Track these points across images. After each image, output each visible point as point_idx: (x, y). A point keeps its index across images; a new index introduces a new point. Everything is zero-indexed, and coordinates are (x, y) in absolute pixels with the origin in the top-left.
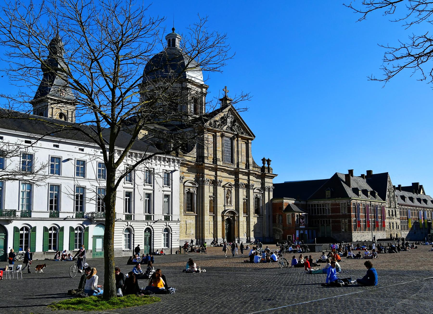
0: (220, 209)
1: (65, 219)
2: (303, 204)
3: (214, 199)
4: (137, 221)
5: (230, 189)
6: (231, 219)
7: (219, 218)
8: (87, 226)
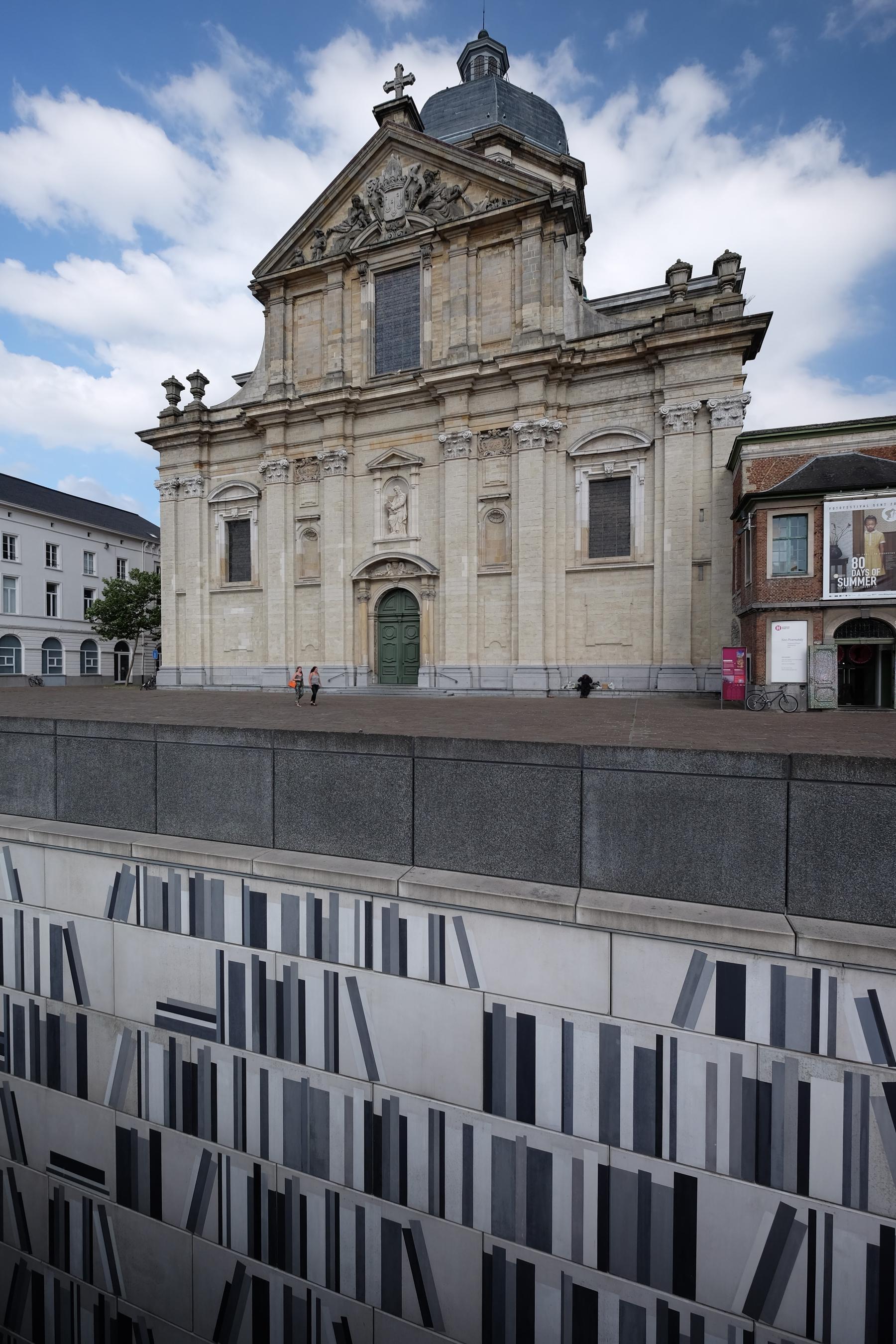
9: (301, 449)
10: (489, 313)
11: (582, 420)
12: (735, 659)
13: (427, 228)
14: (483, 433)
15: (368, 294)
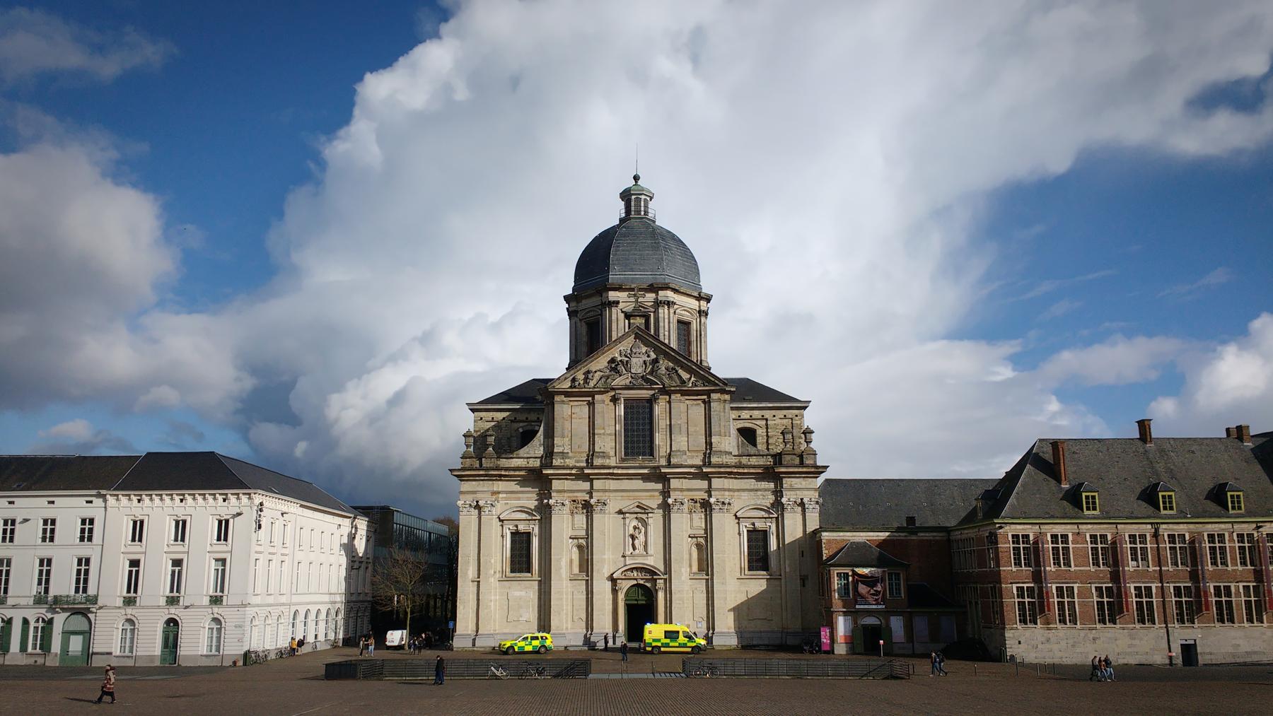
0: (608, 560)
1: (14, 607)
2: (931, 540)
4: (143, 607)
5: (644, 516)
6: (649, 585)
7: (602, 589)
8: (52, 616)
9: (576, 494)
10: (692, 435)
11: (743, 497)
12: (826, 632)
13: (658, 384)
14: (693, 500)
15: (621, 410)
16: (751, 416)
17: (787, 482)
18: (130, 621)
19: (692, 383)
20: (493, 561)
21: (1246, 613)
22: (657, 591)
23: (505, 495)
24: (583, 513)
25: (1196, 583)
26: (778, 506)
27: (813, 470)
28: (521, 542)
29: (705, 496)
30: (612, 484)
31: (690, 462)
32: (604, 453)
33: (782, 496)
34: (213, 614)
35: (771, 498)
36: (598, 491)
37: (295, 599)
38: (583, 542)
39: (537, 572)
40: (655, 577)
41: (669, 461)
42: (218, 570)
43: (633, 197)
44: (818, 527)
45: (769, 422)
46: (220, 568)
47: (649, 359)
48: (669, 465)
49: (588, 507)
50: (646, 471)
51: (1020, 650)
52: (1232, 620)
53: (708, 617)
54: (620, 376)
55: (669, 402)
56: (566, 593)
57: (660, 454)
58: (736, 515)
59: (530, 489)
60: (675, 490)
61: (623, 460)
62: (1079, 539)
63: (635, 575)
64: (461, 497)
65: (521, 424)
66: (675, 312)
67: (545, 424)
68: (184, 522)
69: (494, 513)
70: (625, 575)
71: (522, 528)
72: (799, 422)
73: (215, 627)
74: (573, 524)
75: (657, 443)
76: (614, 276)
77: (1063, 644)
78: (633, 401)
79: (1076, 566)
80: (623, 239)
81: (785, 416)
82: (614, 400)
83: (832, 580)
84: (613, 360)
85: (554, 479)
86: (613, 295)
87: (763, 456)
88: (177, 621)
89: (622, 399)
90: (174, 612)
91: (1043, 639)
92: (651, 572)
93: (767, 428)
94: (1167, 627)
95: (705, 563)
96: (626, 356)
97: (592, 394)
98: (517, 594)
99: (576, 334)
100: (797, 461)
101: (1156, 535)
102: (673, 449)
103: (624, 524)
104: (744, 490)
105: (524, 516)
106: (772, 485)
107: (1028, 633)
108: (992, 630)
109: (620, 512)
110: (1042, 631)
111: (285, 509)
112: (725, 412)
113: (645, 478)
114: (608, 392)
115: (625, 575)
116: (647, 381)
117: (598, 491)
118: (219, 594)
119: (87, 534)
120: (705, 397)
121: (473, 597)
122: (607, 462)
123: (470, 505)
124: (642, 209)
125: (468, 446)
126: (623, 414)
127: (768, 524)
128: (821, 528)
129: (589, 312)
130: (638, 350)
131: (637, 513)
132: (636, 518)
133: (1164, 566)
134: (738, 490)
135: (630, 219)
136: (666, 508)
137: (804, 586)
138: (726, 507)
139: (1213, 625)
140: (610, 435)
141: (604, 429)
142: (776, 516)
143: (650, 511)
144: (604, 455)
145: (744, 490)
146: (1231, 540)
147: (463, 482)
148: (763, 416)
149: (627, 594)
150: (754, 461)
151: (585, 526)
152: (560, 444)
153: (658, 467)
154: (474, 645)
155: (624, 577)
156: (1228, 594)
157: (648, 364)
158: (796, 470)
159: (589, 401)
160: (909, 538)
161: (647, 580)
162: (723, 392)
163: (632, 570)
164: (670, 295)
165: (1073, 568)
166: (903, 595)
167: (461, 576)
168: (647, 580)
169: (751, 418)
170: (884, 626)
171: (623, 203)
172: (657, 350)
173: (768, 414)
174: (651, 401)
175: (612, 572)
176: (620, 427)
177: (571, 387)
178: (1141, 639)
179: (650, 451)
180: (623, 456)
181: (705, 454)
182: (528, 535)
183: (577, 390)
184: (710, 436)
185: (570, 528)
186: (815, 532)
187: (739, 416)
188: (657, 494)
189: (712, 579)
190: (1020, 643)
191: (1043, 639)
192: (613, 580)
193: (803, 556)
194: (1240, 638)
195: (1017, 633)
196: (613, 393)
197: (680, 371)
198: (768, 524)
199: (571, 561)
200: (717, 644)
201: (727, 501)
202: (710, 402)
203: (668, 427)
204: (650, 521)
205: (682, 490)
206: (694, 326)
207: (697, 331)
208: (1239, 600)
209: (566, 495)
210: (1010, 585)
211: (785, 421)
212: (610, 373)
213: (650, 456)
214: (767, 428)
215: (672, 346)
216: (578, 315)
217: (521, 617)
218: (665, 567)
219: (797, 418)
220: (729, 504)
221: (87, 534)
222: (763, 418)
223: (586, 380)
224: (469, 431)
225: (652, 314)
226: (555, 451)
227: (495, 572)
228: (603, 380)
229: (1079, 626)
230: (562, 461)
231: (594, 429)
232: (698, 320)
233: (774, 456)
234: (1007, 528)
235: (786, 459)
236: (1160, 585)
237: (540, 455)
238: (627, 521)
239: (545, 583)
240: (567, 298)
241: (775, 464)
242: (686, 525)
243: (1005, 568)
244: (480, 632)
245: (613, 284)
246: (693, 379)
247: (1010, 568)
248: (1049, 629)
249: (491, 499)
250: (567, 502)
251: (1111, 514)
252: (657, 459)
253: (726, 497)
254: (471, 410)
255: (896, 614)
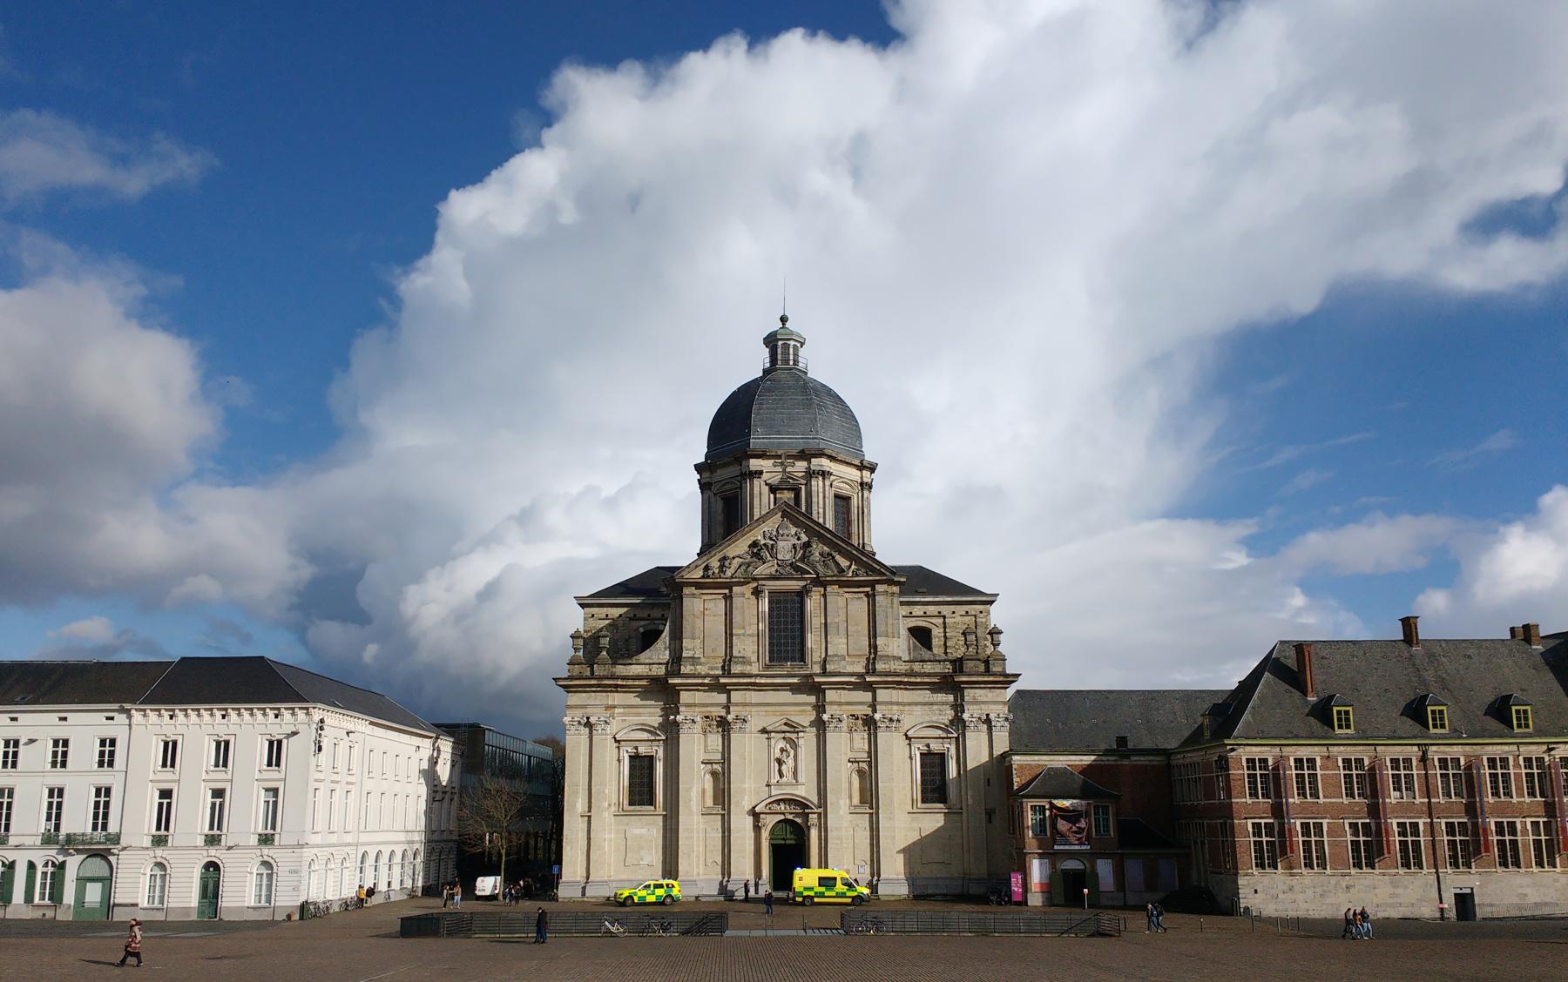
0: (748, 790)
1: (17, 847)
2: (1146, 765)
3: (723, 769)
4: (176, 848)
5: (793, 736)
6: (799, 820)
7: (742, 825)
8: (65, 859)
9: (709, 709)
10: (853, 635)
11: (914, 713)
14: (853, 715)
15: (765, 605)
16: (925, 613)
17: (969, 694)
18: (160, 865)
19: (853, 572)
20: (607, 791)
21: (1535, 855)
22: (809, 828)
23: (622, 710)
24: (718, 732)
25: (1473, 818)
26: (958, 723)
27: (1001, 679)
28: (641, 768)
29: (869, 711)
30: (754, 697)
31: (849, 669)
32: (744, 658)
33: (963, 711)
34: (262, 856)
35: (950, 714)
36: (737, 704)
37: (364, 838)
38: (718, 767)
39: (661, 805)
40: (807, 811)
41: (824, 668)
42: (268, 802)
43: (780, 343)
44: (1008, 749)
45: (947, 620)
46: (271, 800)
47: (799, 542)
48: (824, 673)
49: (724, 725)
50: (795, 680)
51: (1257, 901)
52: (1517, 864)
53: (872, 860)
54: (764, 563)
55: (825, 596)
56: (697, 830)
57: (814, 660)
58: (906, 735)
59: (653, 702)
60: (832, 703)
61: (767, 667)
62: (1329, 764)
63: (783, 808)
64: (568, 712)
65: (642, 623)
66: (831, 484)
67: (671, 622)
68: (227, 743)
69: (608, 732)
70: (770, 809)
71: (643, 750)
72: (984, 620)
73: (265, 872)
74: (706, 746)
75: (809, 646)
76: (757, 440)
77: (1310, 892)
78: (778, 595)
79: (1325, 797)
80: (767, 394)
81: (967, 612)
82: (757, 593)
83: (1025, 814)
84: (755, 544)
85: (682, 690)
86: (755, 464)
87: (939, 661)
88: (218, 865)
89: (767, 592)
90: (215, 854)
91: (1285, 888)
92: (802, 805)
93: (945, 628)
94: (1437, 873)
95: (869, 793)
96: (771, 539)
97: (729, 586)
98: (637, 831)
99: (710, 513)
100: (982, 668)
101: (1424, 759)
102: (829, 654)
103: (769, 746)
104: (916, 704)
105: (645, 736)
106: (951, 698)
107: (1266, 880)
108: (1222, 876)
109: (764, 731)
110: (1283, 878)
111: (351, 727)
112: (892, 608)
113: (795, 689)
114: (749, 583)
115: (770, 809)
116: (797, 569)
117: (737, 704)
118: (269, 831)
119: (107, 758)
120: (868, 589)
121: (582, 836)
122: (747, 669)
123: (579, 722)
124: (791, 357)
125: (576, 650)
126: (767, 610)
127: (946, 746)
128: (1011, 750)
129: (725, 484)
130: (786, 531)
131: (784, 732)
132: (784, 738)
133: (1433, 798)
134: (910, 704)
135: (776, 370)
136: (820, 726)
137: (990, 822)
138: (894, 724)
139: (1495, 870)
140: (751, 635)
141: (743, 628)
142: (956, 735)
143: (801, 729)
144: (744, 661)
145: (916, 704)
146: (1517, 765)
147: (570, 694)
148: (940, 612)
149: (772, 831)
150: (928, 668)
151: (720, 748)
152: (690, 647)
153: (811, 676)
154: (584, 894)
155: (768, 811)
156: (1513, 832)
157: (798, 549)
158: (981, 679)
159: (725, 594)
160: (1119, 763)
161: (797, 815)
162: (891, 582)
163: (778, 802)
164: (825, 464)
165: (1321, 800)
166: (1112, 833)
167: (567, 810)
168: (797, 815)
169: (925, 615)
170: (1088, 870)
171: (768, 350)
172: (810, 531)
173: (946, 610)
174: (802, 594)
175: (754, 805)
176: (764, 626)
177: (703, 577)
178: (1406, 888)
179: (801, 655)
180: (767, 662)
181: (868, 659)
182: (651, 759)
183: (711, 580)
184: (875, 637)
185: (702, 751)
186: (1004, 756)
187: (911, 613)
188: (810, 708)
189: (877, 814)
190: (1256, 892)
191: (1285, 888)
192: (755, 815)
193: (989, 785)
194: (1528, 886)
195: (1252, 880)
196: (755, 585)
197: (838, 558)
198: (946, 746)
199: (704, 791)
200: (883, 894)
201: (895, 718)
202: (874, 595)
203: (823, 626)
204: (801, 742)
205: (840, 704)
206: (855, 502)
207: (858, 508)
208: (1526, 839)
209: (697, 709)
210: (1244, 821)
211: (967, 619)
212: (752, 560)
213: (801, 661)
214: (945, 628)
215: (827, 526)
216: (712, 488)
217: (642, 860)
218: (820, 799)
219: (982, 615)
220: (898, 721)
221: (107, 758)
222: (940, 615)
223: (722, 568)
224: (578, 631)
225: (803, 487)
226: (684, 655)
227: (610, 805)
228: (743, 568)
229: (1328, 871)
230: (693, 668)
231: (731, 629)
232: (860, 494)
233: (953, 662)
234: (1241, 750)
235: (968, 665)
236: (1429, 820)
237: (665, 661)
238: (773, 742)
239: (671, 819)
240: (698, 468)
241: (955, 671)
242: (844, 746)
243: (1237, 800)
244: (591, 879)
245: (755, 450)
246: (853, 567)
247: (1244, 800)
248: (1292, 875)
249: (604, 715)
250: (698, 719)
251: (1369, 733)
252: (810, 666)
253: (894, 711)
254: (579, 604)
255: (1103, 856)
